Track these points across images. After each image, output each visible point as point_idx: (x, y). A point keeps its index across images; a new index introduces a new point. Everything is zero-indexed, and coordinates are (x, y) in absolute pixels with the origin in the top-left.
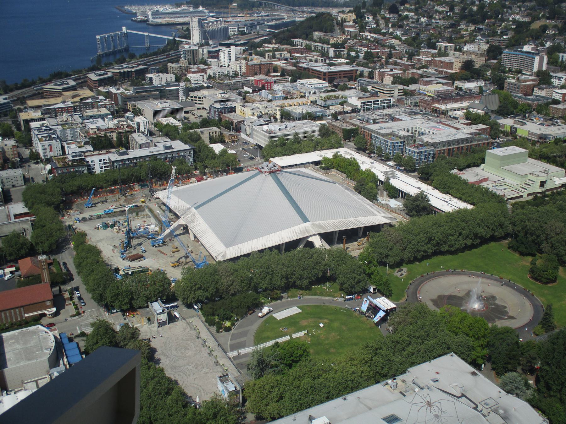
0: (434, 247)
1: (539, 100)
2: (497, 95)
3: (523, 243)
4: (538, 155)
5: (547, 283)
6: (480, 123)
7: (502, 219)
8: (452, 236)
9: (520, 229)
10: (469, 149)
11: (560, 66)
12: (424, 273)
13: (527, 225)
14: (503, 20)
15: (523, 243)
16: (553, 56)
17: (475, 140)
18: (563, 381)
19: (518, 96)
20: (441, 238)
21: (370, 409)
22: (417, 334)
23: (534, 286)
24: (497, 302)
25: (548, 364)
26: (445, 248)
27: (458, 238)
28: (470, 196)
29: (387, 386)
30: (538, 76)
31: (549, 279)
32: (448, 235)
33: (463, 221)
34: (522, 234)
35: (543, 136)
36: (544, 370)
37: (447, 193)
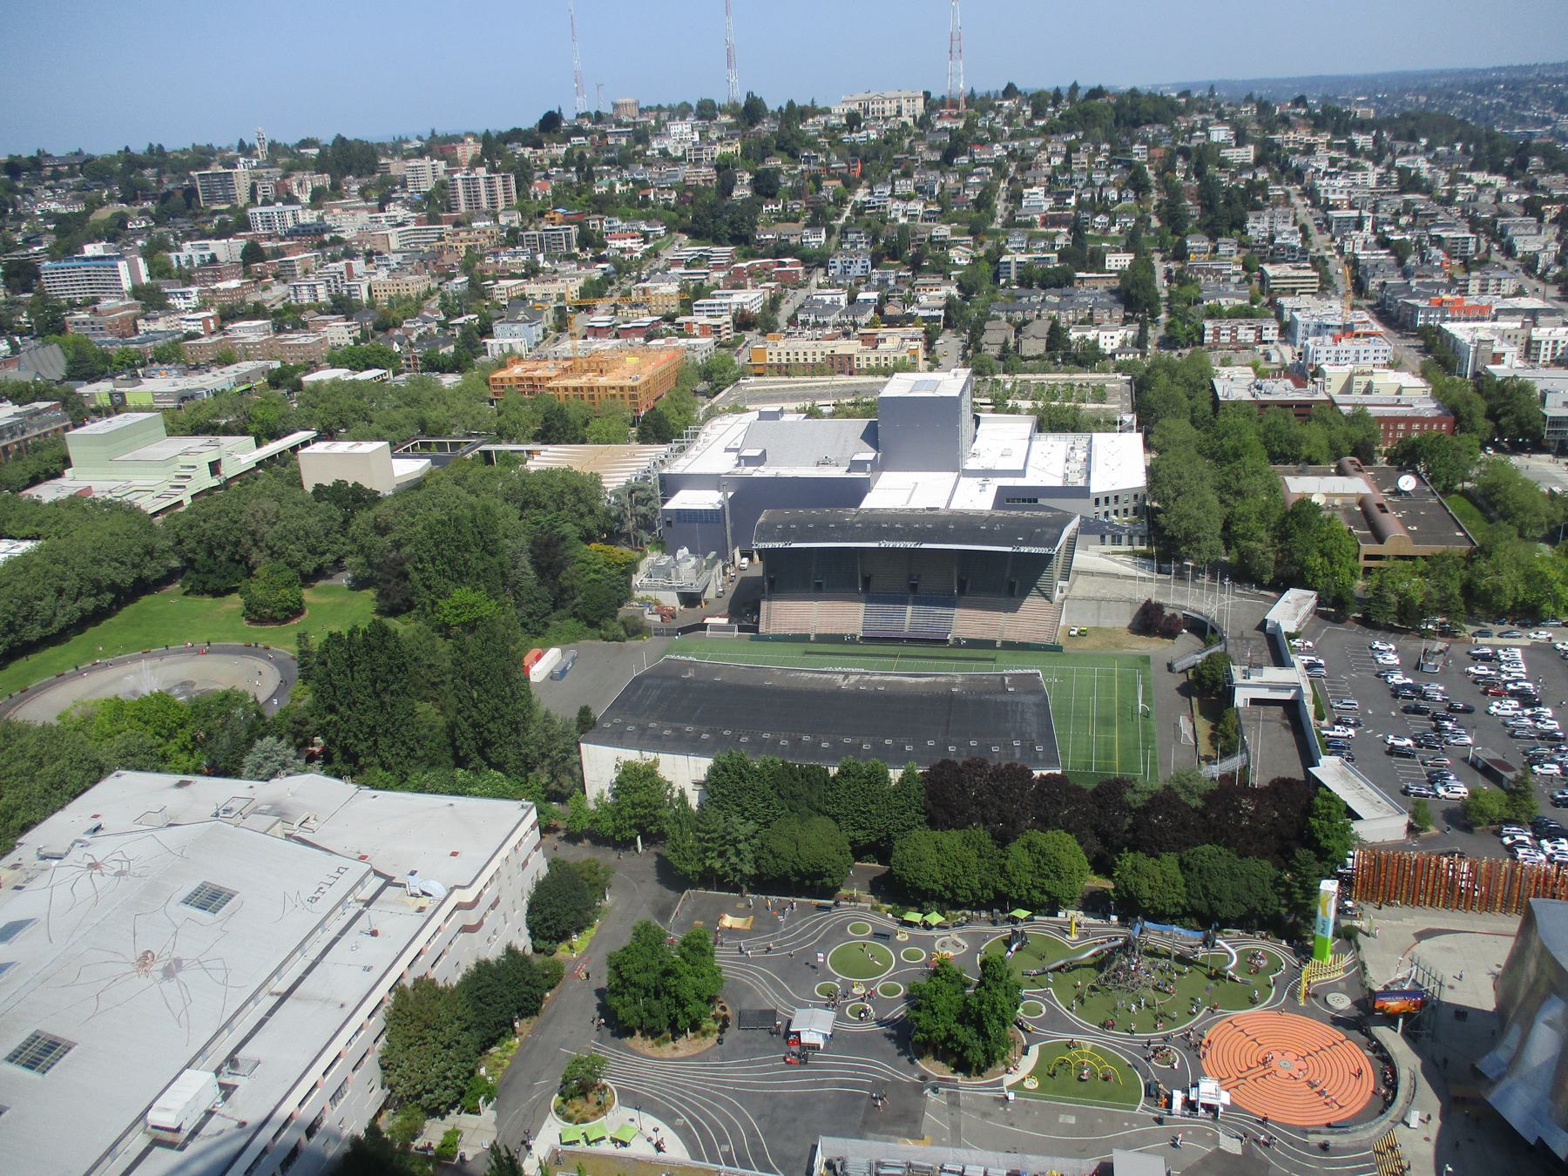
1: (154, 340)
4: (187, 426)
5: (286, 620)
6: (34, 400)
8: (41, 600)
9: (194, 545)
10: (23, 449)
11: (180, 277)
14: (20, 217)
15: (211, 571)
16: (156, 259)
17: (33, 426)
19: (107, 342)
20: (12, 608)
23: (265, 634)
25: (332, 709)
26: (34, 632)
27: (57, 599)
28: (56, 523)
30: (137, 298)
31: (287, 609)
32: (26, 601)
33: (55, 562)
34: (201, 556)
36: (329, 723)
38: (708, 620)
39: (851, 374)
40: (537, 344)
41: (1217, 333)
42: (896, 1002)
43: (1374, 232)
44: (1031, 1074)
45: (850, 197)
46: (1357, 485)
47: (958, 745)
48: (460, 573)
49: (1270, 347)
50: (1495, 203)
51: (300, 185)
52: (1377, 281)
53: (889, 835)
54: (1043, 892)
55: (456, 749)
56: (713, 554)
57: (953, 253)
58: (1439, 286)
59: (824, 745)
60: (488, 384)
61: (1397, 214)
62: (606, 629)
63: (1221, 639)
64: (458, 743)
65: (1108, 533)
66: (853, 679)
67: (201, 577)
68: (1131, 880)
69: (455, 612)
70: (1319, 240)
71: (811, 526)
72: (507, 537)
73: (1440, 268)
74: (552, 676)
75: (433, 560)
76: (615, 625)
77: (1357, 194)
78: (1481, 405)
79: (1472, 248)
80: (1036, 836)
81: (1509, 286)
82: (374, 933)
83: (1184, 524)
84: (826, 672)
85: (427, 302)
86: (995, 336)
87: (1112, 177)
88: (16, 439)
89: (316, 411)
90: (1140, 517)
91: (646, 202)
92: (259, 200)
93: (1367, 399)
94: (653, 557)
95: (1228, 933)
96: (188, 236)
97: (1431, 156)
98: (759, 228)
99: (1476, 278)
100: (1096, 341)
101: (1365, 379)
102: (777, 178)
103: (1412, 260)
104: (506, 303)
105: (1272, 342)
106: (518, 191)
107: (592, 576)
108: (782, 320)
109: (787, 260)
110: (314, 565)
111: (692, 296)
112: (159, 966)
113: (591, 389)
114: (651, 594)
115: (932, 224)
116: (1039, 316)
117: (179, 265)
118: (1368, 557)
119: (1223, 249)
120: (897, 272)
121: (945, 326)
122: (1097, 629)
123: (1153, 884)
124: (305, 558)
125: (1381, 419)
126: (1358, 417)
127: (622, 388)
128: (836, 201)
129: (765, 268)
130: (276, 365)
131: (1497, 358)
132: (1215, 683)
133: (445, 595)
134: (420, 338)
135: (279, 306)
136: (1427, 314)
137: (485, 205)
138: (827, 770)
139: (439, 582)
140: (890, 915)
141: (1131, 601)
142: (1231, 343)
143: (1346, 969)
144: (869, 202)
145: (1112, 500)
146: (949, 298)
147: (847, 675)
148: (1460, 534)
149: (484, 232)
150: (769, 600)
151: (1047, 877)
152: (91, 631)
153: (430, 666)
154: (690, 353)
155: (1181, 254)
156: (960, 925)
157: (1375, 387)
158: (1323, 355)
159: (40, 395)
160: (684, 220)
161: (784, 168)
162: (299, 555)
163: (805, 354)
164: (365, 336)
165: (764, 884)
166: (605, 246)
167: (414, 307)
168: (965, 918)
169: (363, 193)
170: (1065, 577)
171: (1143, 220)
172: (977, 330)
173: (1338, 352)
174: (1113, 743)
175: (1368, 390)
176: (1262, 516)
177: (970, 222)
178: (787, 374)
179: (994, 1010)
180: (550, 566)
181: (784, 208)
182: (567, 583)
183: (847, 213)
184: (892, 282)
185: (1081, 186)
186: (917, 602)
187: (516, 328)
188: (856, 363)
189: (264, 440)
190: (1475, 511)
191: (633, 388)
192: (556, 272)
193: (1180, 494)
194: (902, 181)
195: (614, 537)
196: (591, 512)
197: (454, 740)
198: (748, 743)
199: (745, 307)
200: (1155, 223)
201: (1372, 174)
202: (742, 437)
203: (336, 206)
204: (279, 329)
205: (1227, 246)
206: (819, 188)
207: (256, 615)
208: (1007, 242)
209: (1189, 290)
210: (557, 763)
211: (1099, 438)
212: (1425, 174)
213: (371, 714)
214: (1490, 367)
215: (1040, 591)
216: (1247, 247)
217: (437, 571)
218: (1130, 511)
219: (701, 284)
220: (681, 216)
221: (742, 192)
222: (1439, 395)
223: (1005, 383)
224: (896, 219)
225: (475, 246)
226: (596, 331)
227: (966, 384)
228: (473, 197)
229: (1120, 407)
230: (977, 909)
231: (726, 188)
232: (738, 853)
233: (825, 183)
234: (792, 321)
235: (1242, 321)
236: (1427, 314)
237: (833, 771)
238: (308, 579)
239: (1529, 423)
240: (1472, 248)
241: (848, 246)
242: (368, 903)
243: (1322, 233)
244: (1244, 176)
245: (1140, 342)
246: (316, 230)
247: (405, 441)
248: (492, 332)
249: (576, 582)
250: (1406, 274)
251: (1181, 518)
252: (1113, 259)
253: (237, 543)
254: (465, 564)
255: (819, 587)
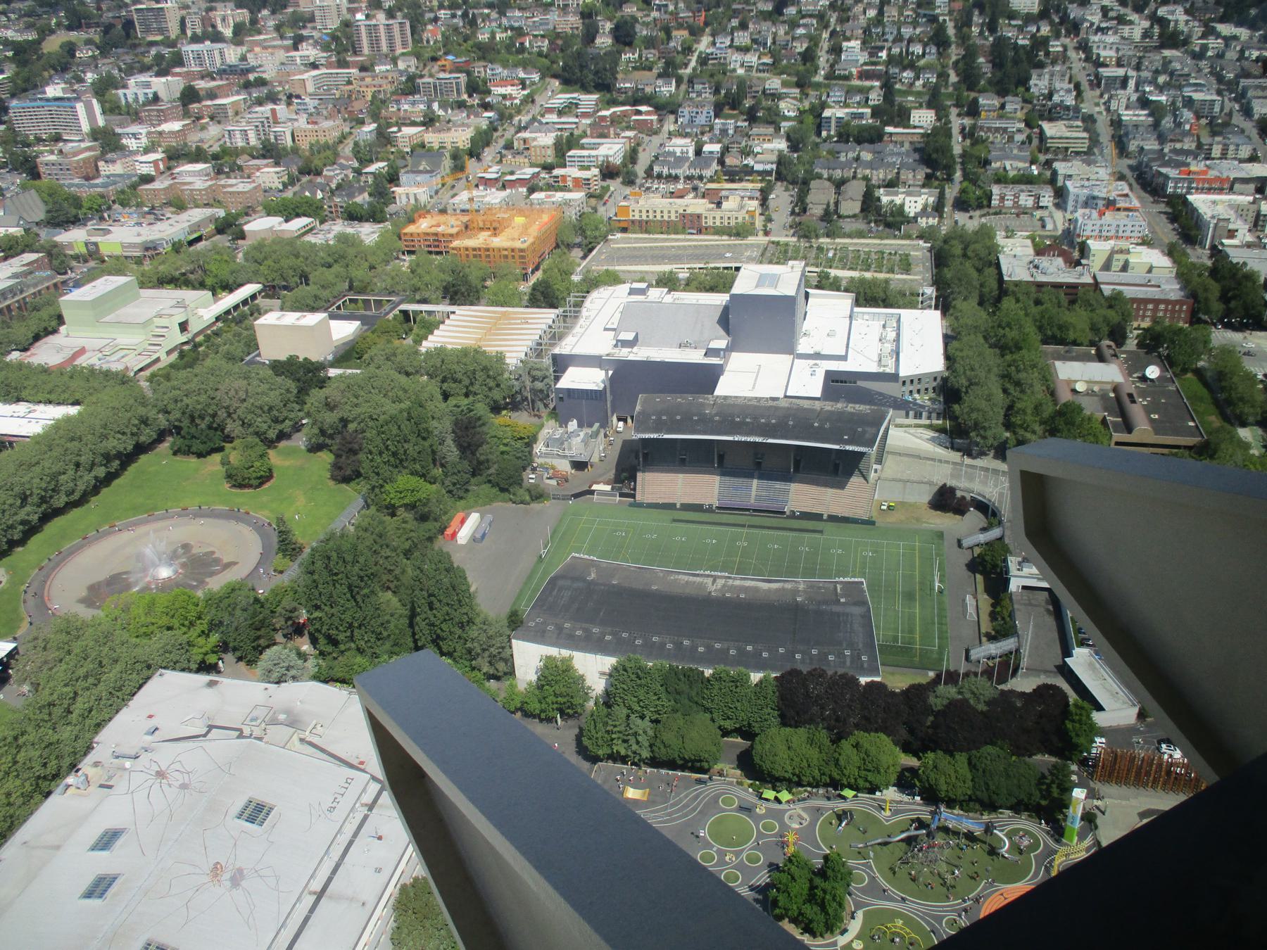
0: (39, 506)
1: (115, 183)
2: (33, 191)
3: (193, 437)
6: (23, 252)
7: (142, 411)
8: (64, 473)
9: (178, 415)
10: (22, 306)
11: (128, 114)
12: (42, 561)
13: (188, 405)
15: (193, 437)
16: (107, 97)
17: (28, 286)
18: (350, 621)
19: (73, 184)
20: (44, 485)
21: (58, 847)
22: (81, 672)
24: (195, 551)
25: (317, 607)
26: (59, 501)
27: (76, 471)
28: (64, 391)
29: (71, 791)
30: (95, 140)
32: (55, 476)
33: (72, 439)
34: (186, 423)
35: (151, 245)
36: (315, 619)
37: (18, 400)
38: (595, 487)
39: (700, 232)
40: (437, 192)
41: (1002, 199)
42: (759, 869)
43: (1137, 90)
44: (858, 937)
45: (695, 46)
46: (1110, 373)
47: (803, 653)
48: (401, 461)
49: (1045, 213)
50: (1238, 60)
51: (223, 20)
52: (1136, 143)
53: (749, 725)
54: (866, 780)
55: (415, 641)
56: (597, 425)
57: (782, 105)
58: (1187, 153)
59: (701, 649)
60: (400, 239)
61: (1157, 72)
62: (514, 494)
63: (1000, 523)
64: (417, 637)
65: (912, 409)
66: (720, 582)
67: (187, 442)
68: (932, 776)
69: (399, 495)
70: (1090, 94)
71: (678, 417)
72: (433, 418)
73: (1189, 133)
74: (474, 539)
75: (381, 453)
76: (521, 492)
77: (1127, 51)
78: (1215, 288)
79: (1217, 109)
80: (860, 736)
81: (1245, 152)
82: (380, 838)
83: (974, 416)
84: (698, 575)
85: (341, 146)
86: (820, 196)
87: (918, 31)
88: (16, 298)
89: (261, 268)
90: (939, 395)
91: (522, 49)
92: (189, 33)
93: (1124, 277)
94: (550, 429)
95: (1001, 813)
96: (130, 71)
97: (1188, 6)
98: (620, 76)
99: (1218, 143)
100: (902, 205)
101: (1122, 257)
102: (633, 27)
103: (1167, 122)
104: (408, 150)
105: (1047, 207)
106: (412, 35)
107: (502, 448)
108: (640, 169)
109: (644, 108)
110: (277, 431)
111: (564, 146)
112: (227, 876)
113: (488, 250)
114: (548, 460)
115: (766, 75)
116: (854, 177)
117: (127, 102)
118: (1117, 444)
119: (1009, 107)
120: (736, 122)
121: (776, 179)
122: (902, 504)
123: (948, 780)
124: (270, 427)
125: (1134, 300)
126: (1115, 301)
127: (513, 250)
128: (684, 49)
129: (625, 114)
130: (221, 213)
131: (1232, 234)
132: (995, 566)
133: (392, 480)
134: (339, 187)
135: (216, 148)
136: (1176, 183)
137: (385, 49)
138: (703, 672)
139: (385, 471)
140: (751, 790)
141: (930, 483)
142: (1013, 207)
143: (1087, 850)
144: (712, 54)
145: (916, 382)
146: (780, 152)
147: (715, 578)
148: (1191, 424)
149: (386, 78)
150: (644, 472)
151: (869, 771)
152: (105, 491)
153: (386, 558)
154: (565, 208)
155: (973, 110)
156: (804, 799)
157: (1131, 265)
158: (1089, 228)
159: (28, 248)
160: (555, 66)
161: (639, 15)
162: (265, 426)
163: (662, 212)
164: (292, 181)
165: (655, 762)
166: (489, 92)
167: (329, 152)
168: (807, 794)
169: (278, 28)
170: (879, 461)
171: (943, 76)
172: (803, 186)
173: (1101, 226)
174: (915, 617)
175: (1125, 268)
176: (1037, 408)
177: (797, 74)
178: (647, 232)
179: (834, 900)
180: (469, 445)
181: (640, 56)
182: (482, 458)
183: (693, 64)
184: (731, 132)
185: (890, 38)
186: (761, 477)
187: (419, 178)
188: (704, 220)
189: (219, 291)
190: (1204, 392)
191: (522, 250)
192: (449, 121)
193: (971, 384)
194: (741, 33)
195: (515, 406)
196: (498, 385)
197: (414, 634)
198: (642, 645)
199: (610, 159)
200: (953, 78)
201: (1138, 25)
202: (618, 316)
203: (258, 43)
204: (219, 172)
205: (1013, 104)
206: (669, 37)
207: (239, 480)
208: (828, 96)
209: (980, 151)
210: (495, 656)
211: (907, 314)
212: (1181, 26)
213: (349, 613)
214: (1225, 241)
215: (862, 473)
216: (1030, 102)
217: (385, 463)
218: (931, 390)
219: (572, 134)
220: (553, 62)
221: (604, 41)
222: (1184, 276)
223: (828, 250)
224: (734, 70)
225: (380, 91)
226: (487, 182)
227: (800, 280)
228: (375, 43)
229: (921, 279)
230: (817, 786)
231: (590, 36)
232: (638, 743)
233: (675, 33)
234: (649, 173)
235: (1023, 187)
236: (1176, 183)
237: (708, 672)
238: (271, 444)
239: (1253, 308)
240: (1217, 109)
241: (694, 95)
242: (371, 807)
243: (1092, 89)
244: (1029, 29)
245: (938, 208)
246: (242, 70)
247: (337, 298)
248: (398, 179)
249: (490, 457)
250: (1162, 139)
251: (972, 410)
252: (917, 116)
253: (214, 415)
254: (405, 451)
255: (683, 462)
